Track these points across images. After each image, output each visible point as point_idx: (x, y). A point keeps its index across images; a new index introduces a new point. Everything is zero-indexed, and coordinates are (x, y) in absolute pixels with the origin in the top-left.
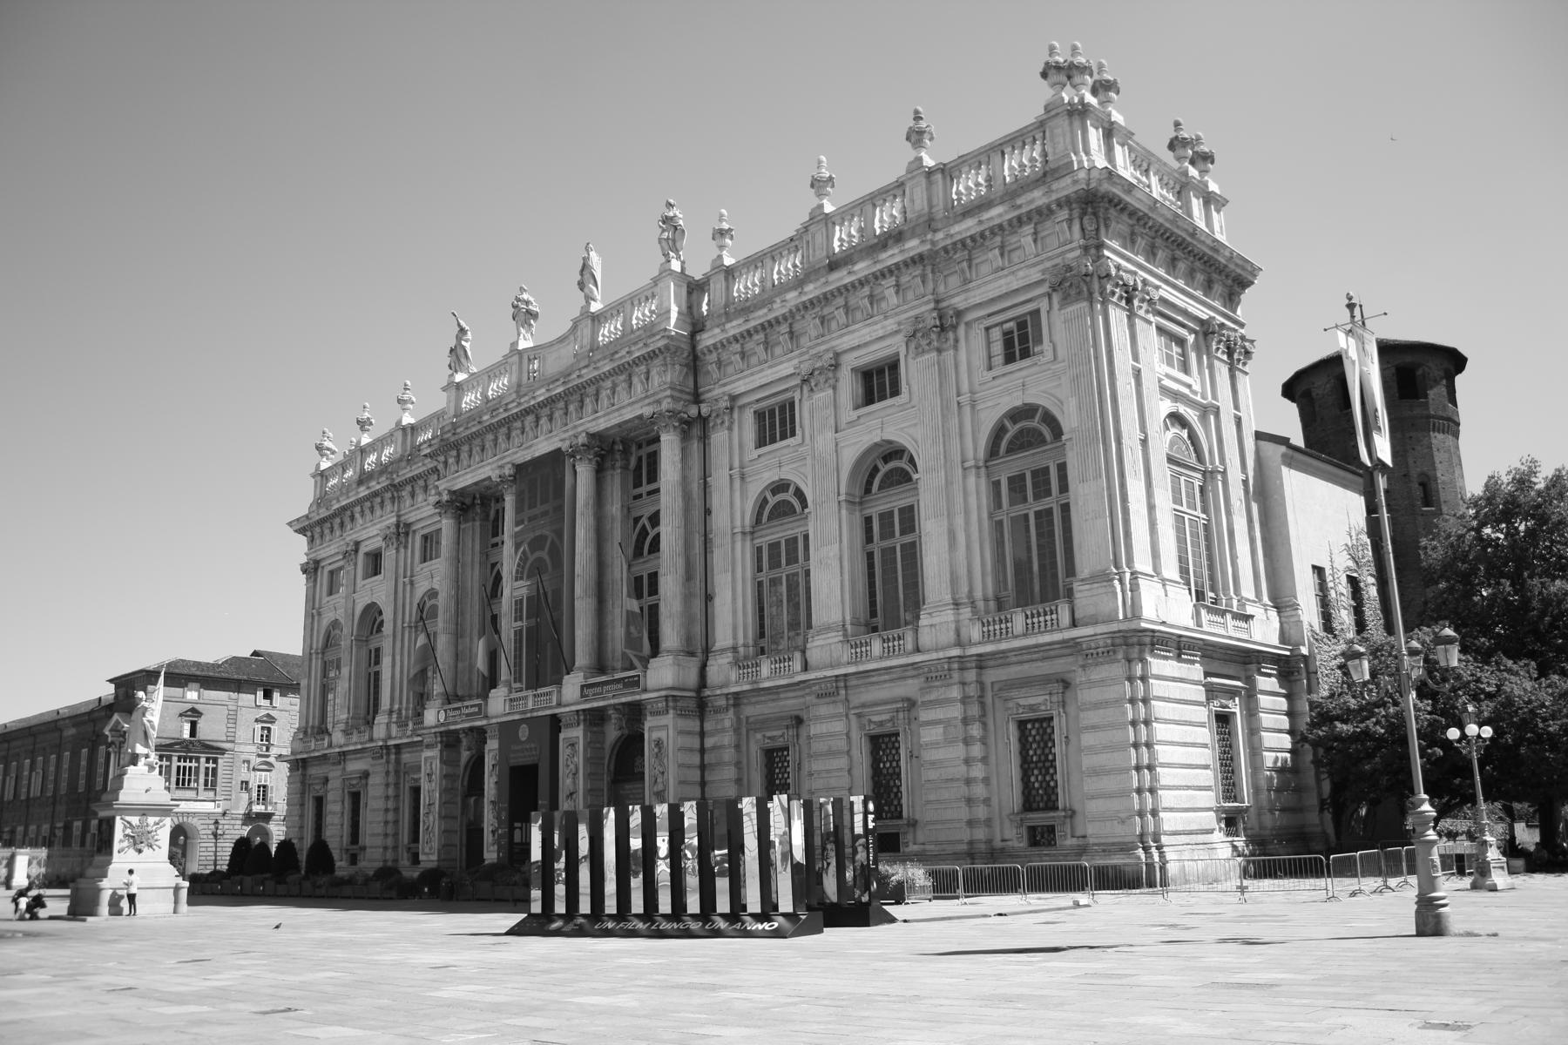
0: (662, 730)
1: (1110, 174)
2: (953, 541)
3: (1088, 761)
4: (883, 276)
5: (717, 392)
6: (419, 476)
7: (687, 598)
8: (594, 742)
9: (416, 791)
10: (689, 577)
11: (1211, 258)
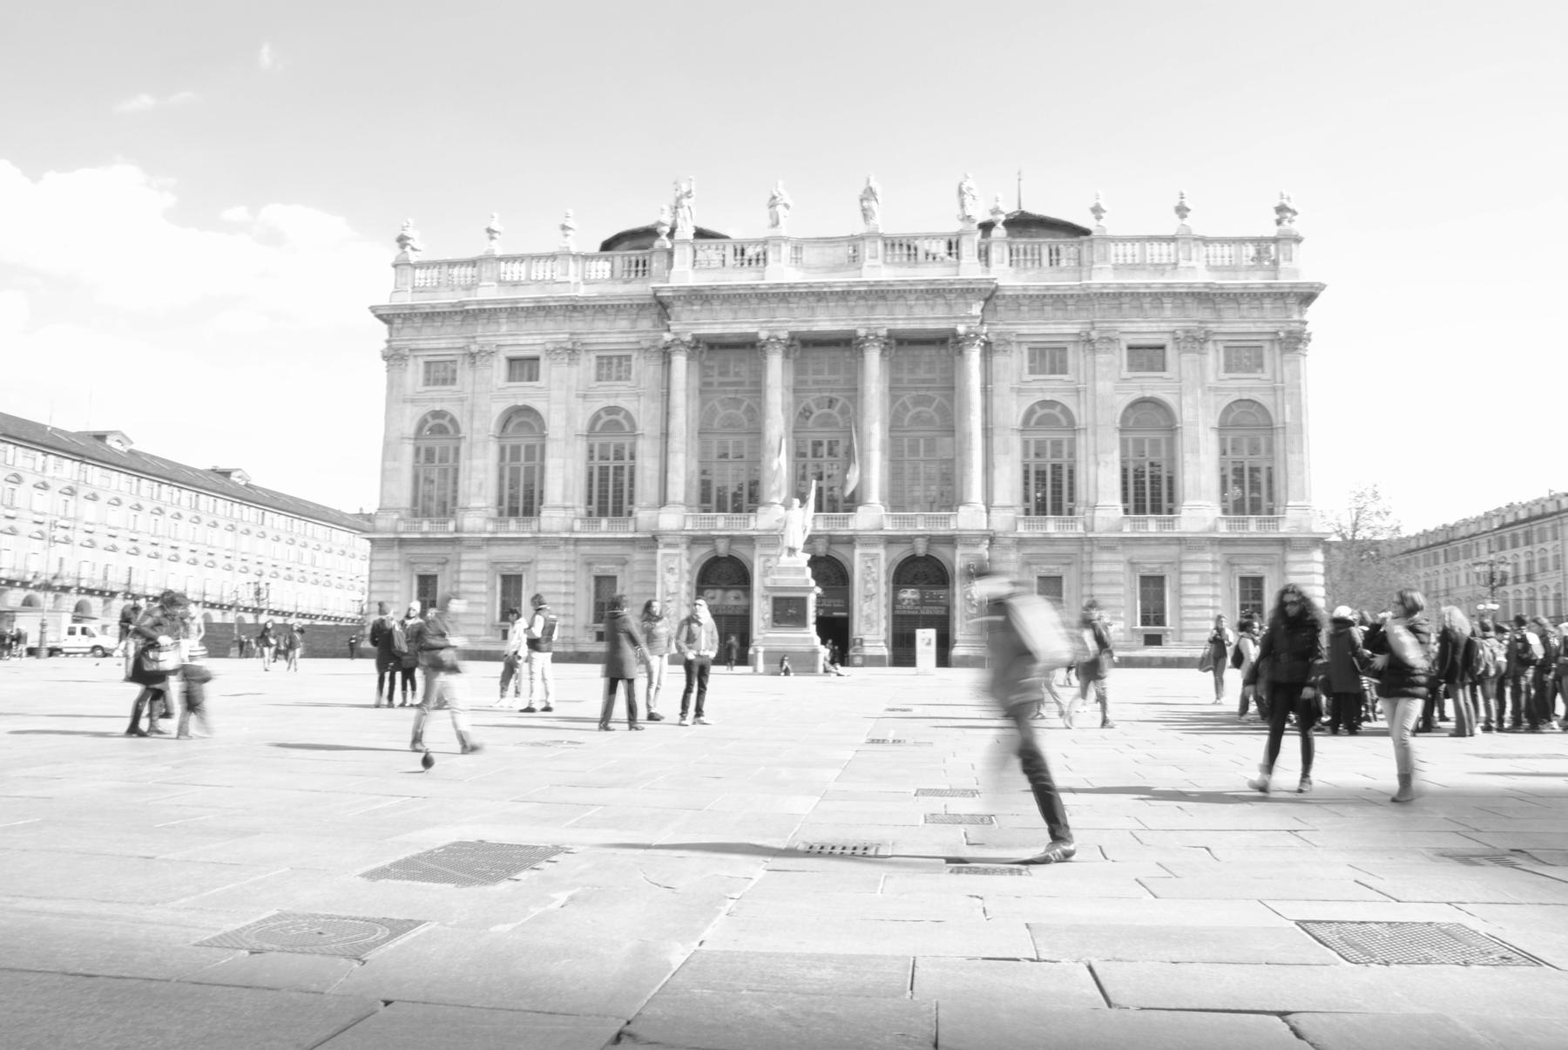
5: (1000, 327)
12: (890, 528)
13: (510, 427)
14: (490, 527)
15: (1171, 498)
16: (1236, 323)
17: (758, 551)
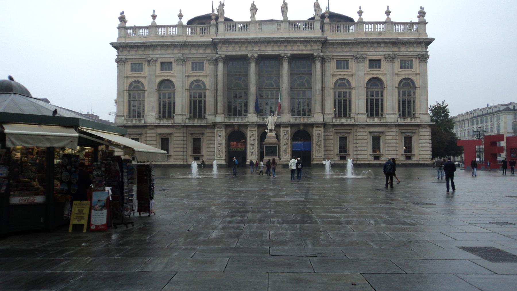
5: (327, 53)
12: (293, 121)
13: (162, 88)
14: (157, 122)
15: (382, 111)
16: (405, 51)
17: (249, 129)
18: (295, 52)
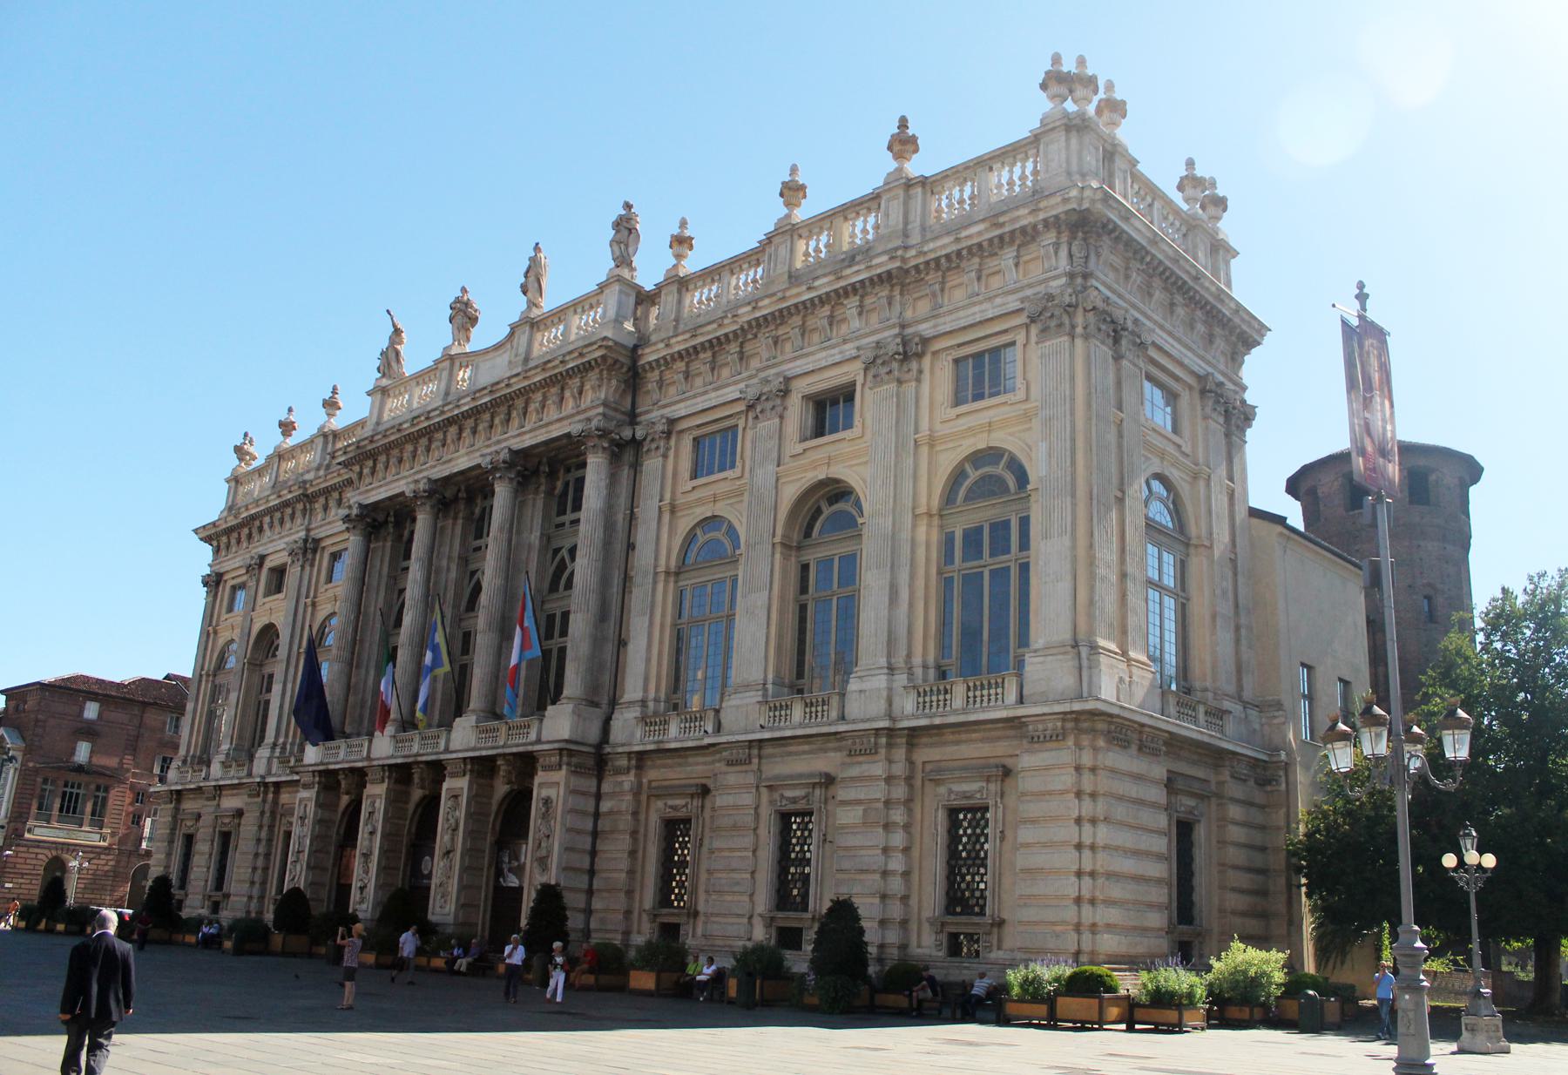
0: (551, 786)
1: (1107, 198)
2: (894, 598)
3: (1022, 860)
4: (846, 295)
6: (333, 488)
7: (597, 642)
8: (479, 796)
9: (288, 834)
10: (602, 616)
11: (1213, 307)
18: (528, 441)
